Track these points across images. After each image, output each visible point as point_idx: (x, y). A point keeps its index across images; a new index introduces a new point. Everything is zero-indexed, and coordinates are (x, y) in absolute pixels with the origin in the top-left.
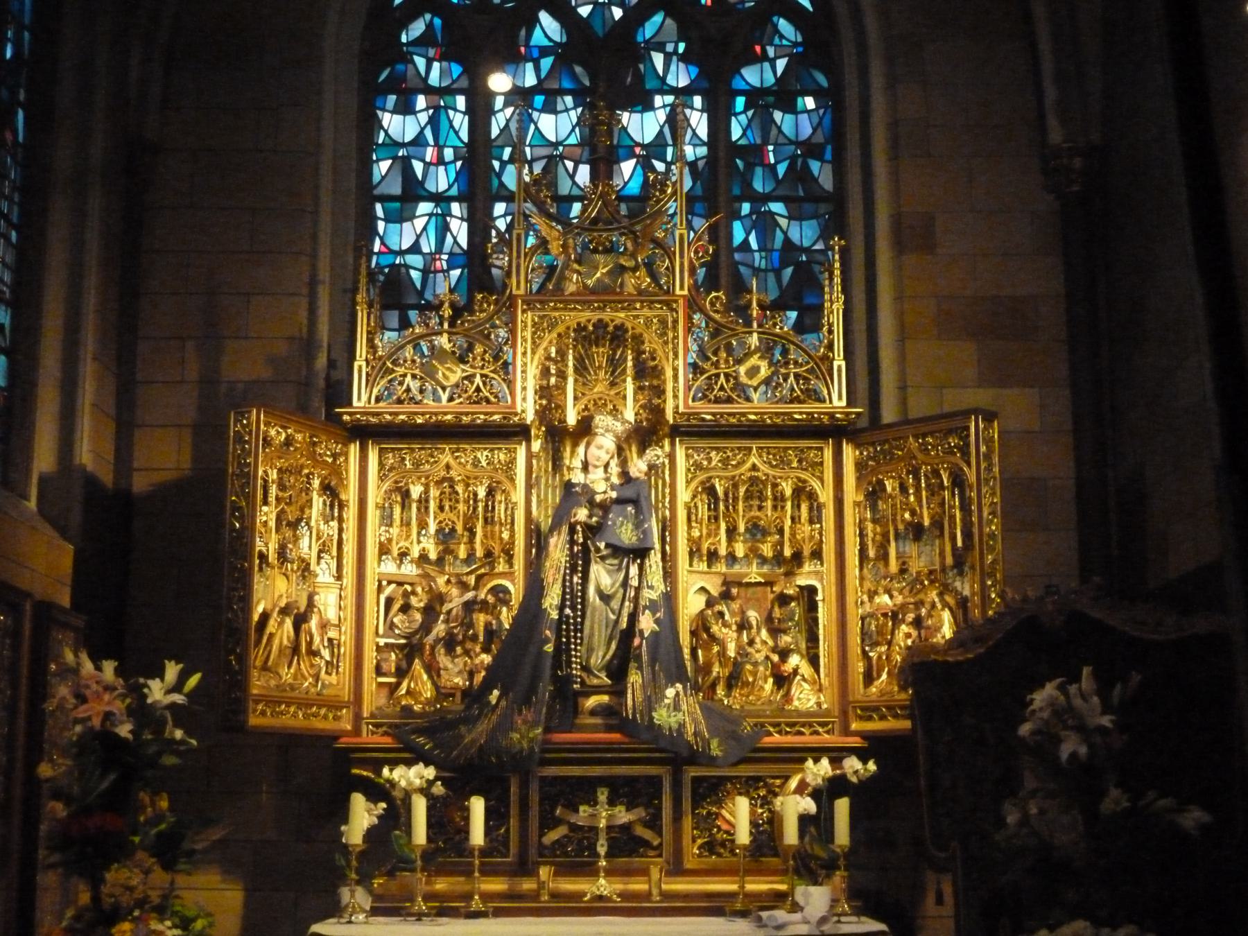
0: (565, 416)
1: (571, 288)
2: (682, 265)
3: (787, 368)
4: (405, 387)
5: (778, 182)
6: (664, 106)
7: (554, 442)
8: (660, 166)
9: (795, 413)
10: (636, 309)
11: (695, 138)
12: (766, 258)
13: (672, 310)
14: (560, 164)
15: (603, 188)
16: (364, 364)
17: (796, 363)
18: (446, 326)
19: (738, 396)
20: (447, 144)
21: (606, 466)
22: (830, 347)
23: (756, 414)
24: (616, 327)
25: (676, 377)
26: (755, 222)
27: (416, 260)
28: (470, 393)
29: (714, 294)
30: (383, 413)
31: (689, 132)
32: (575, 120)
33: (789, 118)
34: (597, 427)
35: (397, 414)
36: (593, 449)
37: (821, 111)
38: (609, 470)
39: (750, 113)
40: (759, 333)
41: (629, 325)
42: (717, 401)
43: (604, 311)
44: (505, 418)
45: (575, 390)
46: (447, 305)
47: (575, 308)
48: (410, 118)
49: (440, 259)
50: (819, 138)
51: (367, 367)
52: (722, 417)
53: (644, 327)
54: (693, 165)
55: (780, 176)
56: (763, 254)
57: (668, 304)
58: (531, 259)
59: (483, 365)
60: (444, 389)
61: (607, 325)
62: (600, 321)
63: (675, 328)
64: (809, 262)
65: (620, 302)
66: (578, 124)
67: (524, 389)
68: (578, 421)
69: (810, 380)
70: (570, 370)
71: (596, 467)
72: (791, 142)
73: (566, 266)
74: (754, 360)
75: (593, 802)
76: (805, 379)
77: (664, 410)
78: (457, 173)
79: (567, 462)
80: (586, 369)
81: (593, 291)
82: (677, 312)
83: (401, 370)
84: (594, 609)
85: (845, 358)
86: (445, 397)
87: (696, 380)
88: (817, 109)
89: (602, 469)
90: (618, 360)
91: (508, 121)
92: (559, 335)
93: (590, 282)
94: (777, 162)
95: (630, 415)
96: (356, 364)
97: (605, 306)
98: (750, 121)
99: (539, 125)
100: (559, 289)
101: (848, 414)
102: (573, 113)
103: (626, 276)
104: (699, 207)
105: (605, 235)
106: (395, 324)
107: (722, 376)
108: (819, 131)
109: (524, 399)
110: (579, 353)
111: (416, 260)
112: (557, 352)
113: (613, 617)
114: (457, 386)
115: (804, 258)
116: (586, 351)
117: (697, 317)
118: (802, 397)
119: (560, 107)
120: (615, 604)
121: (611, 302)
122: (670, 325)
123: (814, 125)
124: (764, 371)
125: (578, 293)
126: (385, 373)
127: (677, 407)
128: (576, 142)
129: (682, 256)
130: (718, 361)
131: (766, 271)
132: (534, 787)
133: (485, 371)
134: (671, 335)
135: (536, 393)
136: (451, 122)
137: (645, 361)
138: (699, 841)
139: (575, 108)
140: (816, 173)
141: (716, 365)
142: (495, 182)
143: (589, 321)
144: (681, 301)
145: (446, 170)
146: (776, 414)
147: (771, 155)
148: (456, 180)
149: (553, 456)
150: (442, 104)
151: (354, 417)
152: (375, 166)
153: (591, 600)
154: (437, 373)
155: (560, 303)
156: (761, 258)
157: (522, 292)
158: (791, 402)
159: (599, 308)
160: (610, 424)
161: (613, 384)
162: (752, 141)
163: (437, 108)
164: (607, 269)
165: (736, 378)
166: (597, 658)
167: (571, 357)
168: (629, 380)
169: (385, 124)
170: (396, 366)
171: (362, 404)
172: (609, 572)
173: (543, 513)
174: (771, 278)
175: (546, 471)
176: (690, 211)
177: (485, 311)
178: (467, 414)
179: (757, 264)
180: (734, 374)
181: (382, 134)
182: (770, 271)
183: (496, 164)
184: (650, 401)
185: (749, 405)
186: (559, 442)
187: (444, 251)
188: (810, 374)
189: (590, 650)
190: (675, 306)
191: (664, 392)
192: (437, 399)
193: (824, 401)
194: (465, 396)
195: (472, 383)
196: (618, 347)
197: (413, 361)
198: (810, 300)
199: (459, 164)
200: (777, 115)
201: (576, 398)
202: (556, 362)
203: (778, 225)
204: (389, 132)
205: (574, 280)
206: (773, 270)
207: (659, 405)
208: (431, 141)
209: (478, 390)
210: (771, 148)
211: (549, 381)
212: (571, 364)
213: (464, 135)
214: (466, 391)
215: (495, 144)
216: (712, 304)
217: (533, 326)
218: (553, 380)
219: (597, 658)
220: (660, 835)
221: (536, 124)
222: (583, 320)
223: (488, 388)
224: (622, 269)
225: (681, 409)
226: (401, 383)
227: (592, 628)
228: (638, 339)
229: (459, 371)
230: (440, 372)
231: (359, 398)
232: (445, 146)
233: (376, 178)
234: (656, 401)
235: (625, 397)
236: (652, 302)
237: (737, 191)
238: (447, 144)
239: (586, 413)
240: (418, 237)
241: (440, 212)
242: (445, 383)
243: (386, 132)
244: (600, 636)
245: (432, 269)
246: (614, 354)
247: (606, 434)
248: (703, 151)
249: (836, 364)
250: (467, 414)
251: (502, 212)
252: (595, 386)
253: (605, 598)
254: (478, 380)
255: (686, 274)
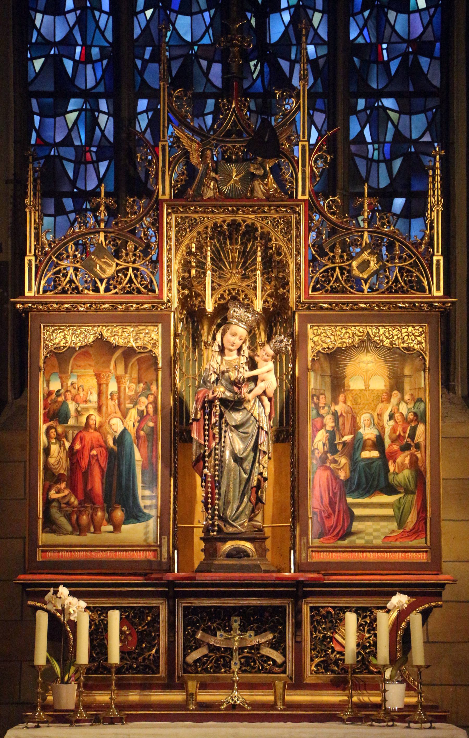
0: (204, 303)
1: (209, 194)
2: (304, 172)
3: (393, 263)
4: (68, 279)
5: (391, 79)
6: (289, 8)
7: (193, 322)
8: (285, 65)
9: (399, 302)
10: (265, 212)
11: (316, 36)
12: (378, 149)
13: (295, 212)
14: (196, 63)
15: (236, 104)
16: (33, 258)
17: (400, 258)
18: (102, 226)
19: (352, 287)
20: (94, 44)
21: (239, 350)
22: (431, 244)
23: (365, 303)
24: (247, 226)
25: (298, 271)
26: (369, 116)
27: (69, 153)
28: (124, 284)
29: (331, 198)
30: (50, 302)
31: (312, 34)
32: (208, 20)
33: (402, 17)
34: (233, 317)
35: (63, 303)
36: (228, 336)
37: (432, 10)
38: (242, 353)
39: (366, 13)
40: (369, 232)
41: (258, 225)
42: (334, 291)
43: (237, 213)
44: (153, 307)
45: (212, 282)
46: (102, 208)
47: (212, 211)
48: (59, 19)
49: (90, 151)
50: (429, 36)
51: (36, 261)
52: (337, 305)
53: (271, 227)
54: (313, 63)
55: (393, 73)
56: (376, 146)
57: (292, 208)
58: (174, 168)
59: (135, 260)
60: (101, 280)
61: (240, 225)
62: (234, 221)
63: (298, 229)
64: (417, 153)
65: (251, 206)
66: (211, 25)
67: (170, 281)
68: (215, 308)
69: (413, 272)
70: (209, 265)
71: (231, 350)
72: (403, 40)
73: (205, 174)
74: (365, 256)
75: (229, 629)
76: (408, 271)
77: (288, 298)
78: (104, 71)
79: (205, 339)
80: (221, 260)
81: (227, 197)
82: (299, 215)
83: (64, 264)
84: (229, 471)
85: (442, 254)
86: (102, 288)
87: (316, 273)
88: (427, 9)
89: (235, 352)
90: (249, 252)
91: (148, 22)
92: (199, 233)
93: (226, 189)
94: (390, 60)
95: (258, 305)
96: (27, 259)
97: (238, 209)
98: (366, 21)
99: (177, 26)
100: (199, 194)
101: (444, 303)
102: (206, 14)
103: (256, 183)
104: (320, 103)
105: (238, 145)
106: (52, 211)
107: (337, 269)
108: (430, 29)
109: (170, 290)
110: (215, 246)
111: (69, 153)
112: (196, 248)
113: (245, 476)
114: (112, 278)
115: (413, 150)
116: (221, 245)
117: (316, 217)
118: (405, 288)
119: (195, 9)
120: (247, 465)
121: (243, 206)
122: (294, 225)
123: (425, 25)
124: (374, 266)
125: (214, 199)
126: (50, 266)
127: (300, 297)
128: (210, 42)
129: (304, 166)
130: (334, 257)
131: (378, 161)
132: (180, 615)
133: (136, 265)
134: (294, 234)
135: (179, 283)
136: (97, 22)
137: (272, 255)
138: (317, 660)
139: (208, 10)
140: (425, 70)
141: (332, 260)
142: (139, 79)
143: (224, 221)
144: (303, 206)
145: (93, 68)
146: (383, 303)
147: (385, 52)
148: (102, 77)
149: (193, 335)
150: (88, 4)
151: (26, 306)
152: (29, 63)
153: (227, 462)
154: (96, 267)
155: (200, 207)
156: (374, 150)
157: (167, 197)
158: (396, 292)
159: (233, 211)
160: (243, 314)
161: (245, 277)
162: (368, 41)
163: (84, 9)
164: (239, 176)
165: (349, 272)
166: (232, 510)
167: (209, 253)
168: (258, 272)
169: (38, 23)
170: (61, 260)
171: (32, 294)
172: (242, 439)
173: (184, 383)
174: (383, 166)
175: (187, 347)
176: (312, 107)
177: (135, 213)
178: (121, 303)
179: (370, 156)
180: (347, 268)
181: (35, 34)
182: (382, 161)
183: (139, 63)
184: (276, 290)
185: (360, 295)
186: (198, 322)
187: (94, 143)
188: (412, 267)
189: (227, 503)
190: (297, 209)
191: (287, 283)
192: (97, 290)
193: (424, 291)
194: (120, 287)
195: (126, 276)
196: (249, 241)
197: (75, 256)
198: (416, 187)
199: (105, 62)
200: (392, 15)
201: (213, 289)
202: (195, 255)
203: (389, 118)
204: (42, 31)
205: (212, 186)
206: (385, 161)
207: (284, 293)
208: (80, 42)
209: (131, 281)
210: (384, 46)
211: (190, 272)
212: (209, 259)
213: (109, 35)
214: (120, 283)
215: (136, 44)
216: (329, 207)
217: (176, 226)
218: (193, 272)
219: (232, 510)
220: (285, 656)
221: (173, 25)
222: (219, 221)
223: (139, 280)
224: (253, 176)
225: (303, 299)
226: (65, 276)
227: (228, 486)
228: (266, 238)
229: (114, 265)
230: (98, 268)
231: (30, 289)
232: (92, 46)
233: (31, 75)
234: (281, 291)
235: (255, 289)
236: (278, 206)
237: (354, 88)
238: (94, 44)
239: (222, 302)
240: (70, 130)
241: (88, 107)
242: (103, 276)
243: (39, 31)
244: (234, 492)
245: (83, 160)
246: (246, 247)
247: (240, 324)
248: (324, 51)
249: (435, 258)
250: (121, 303)
251: (144, 108)
252: (229, 279)
253: (238, 460)
254: (130, 272)
255: (308, 181)
